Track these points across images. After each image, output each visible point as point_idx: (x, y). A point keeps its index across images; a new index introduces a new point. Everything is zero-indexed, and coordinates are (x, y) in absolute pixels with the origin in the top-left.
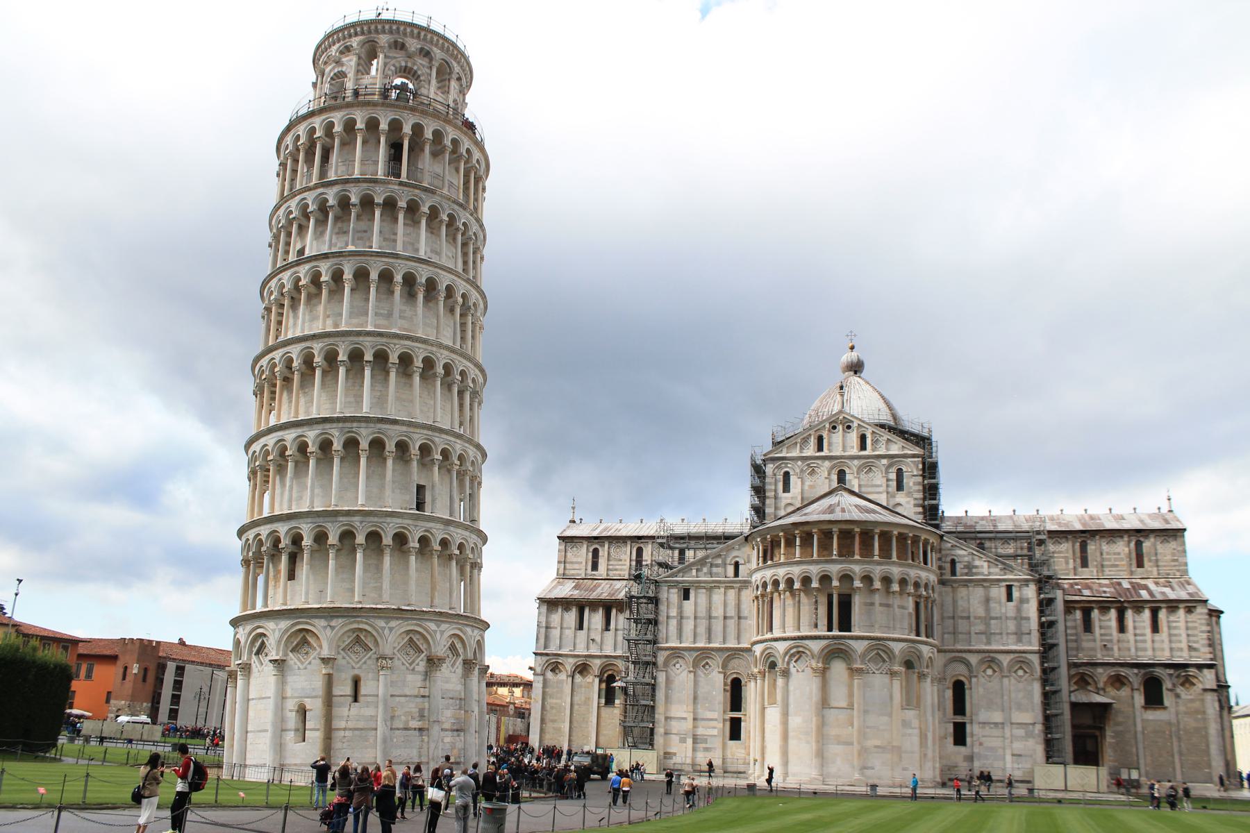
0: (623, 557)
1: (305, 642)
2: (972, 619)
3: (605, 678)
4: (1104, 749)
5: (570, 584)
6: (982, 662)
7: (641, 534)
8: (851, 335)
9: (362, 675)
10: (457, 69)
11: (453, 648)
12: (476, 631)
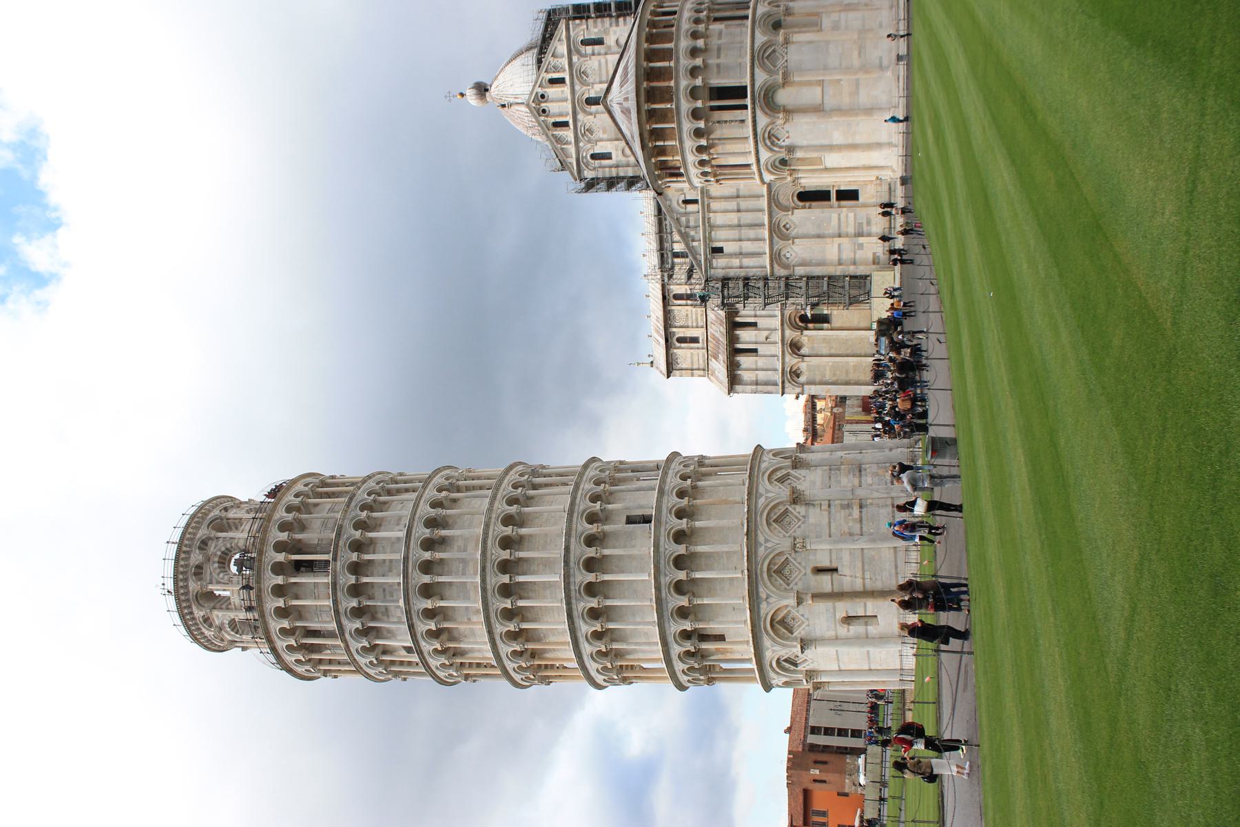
0: (684, 313)
1: (783, 622)
5: (713, 363)
7: (660, 296)
8: (449, 96)
10: (216, 512)
11: (781, 480)
12: (765, 458)
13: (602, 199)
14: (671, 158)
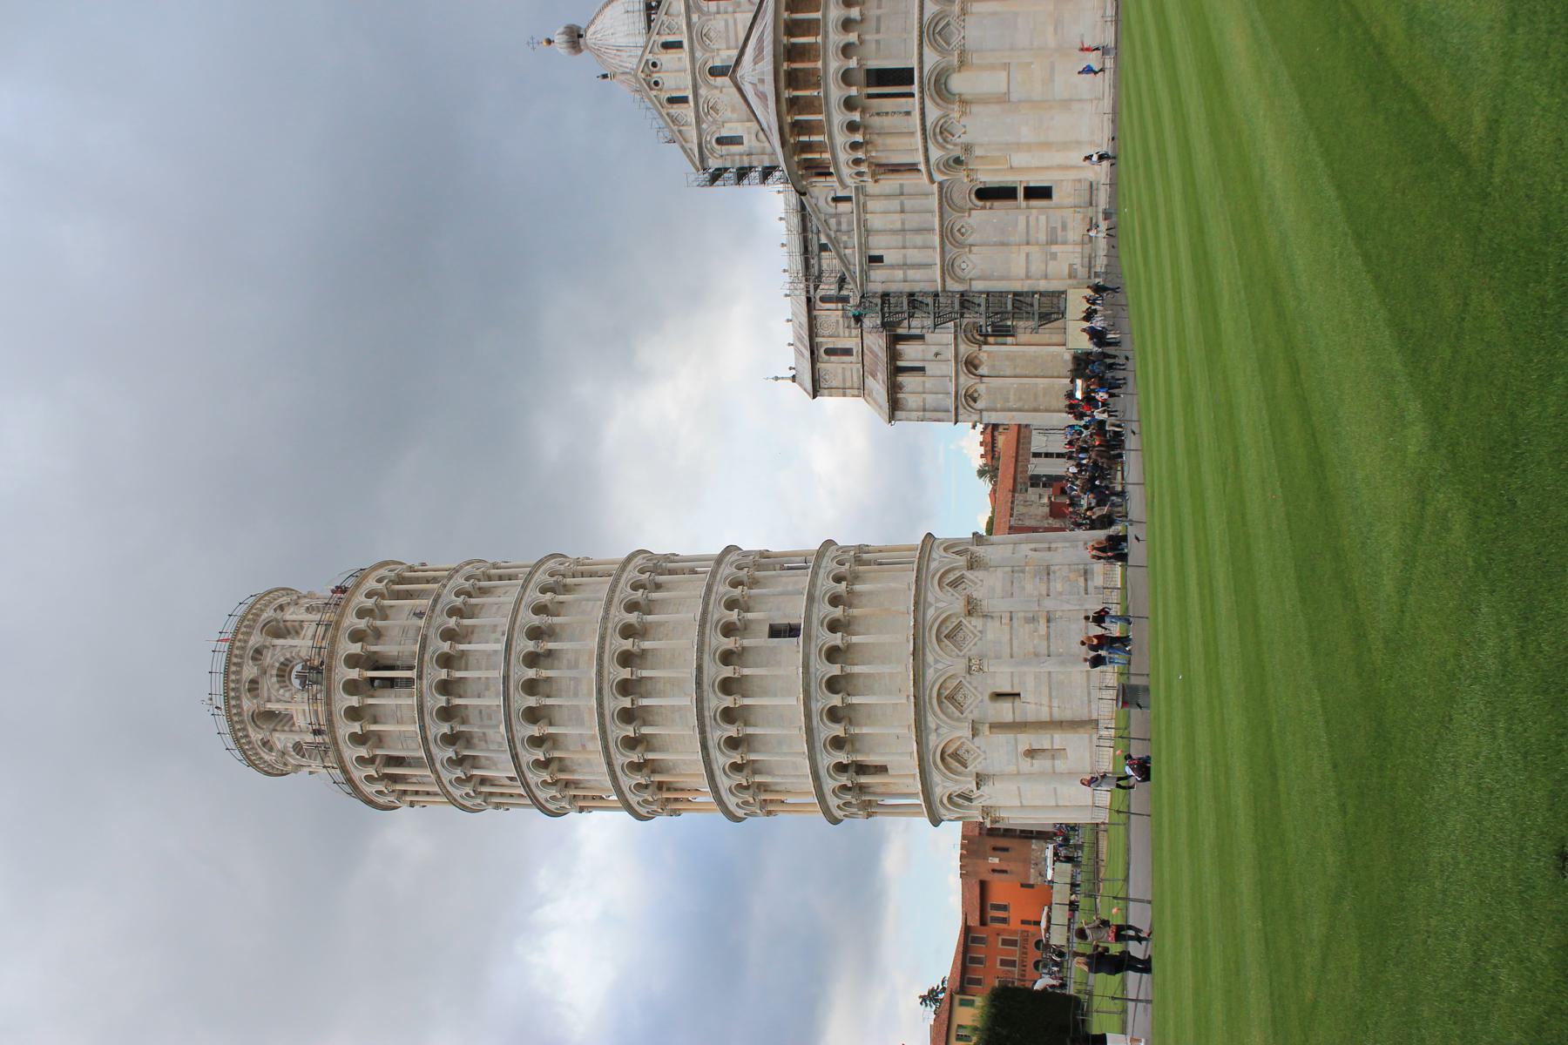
0: (833, 319)
3: (982, 338)
5: (870, 381)
9: (990, 691)
10: (269, 614)
11: (954, 584)
12: (934, 555)
13: (725, 191)
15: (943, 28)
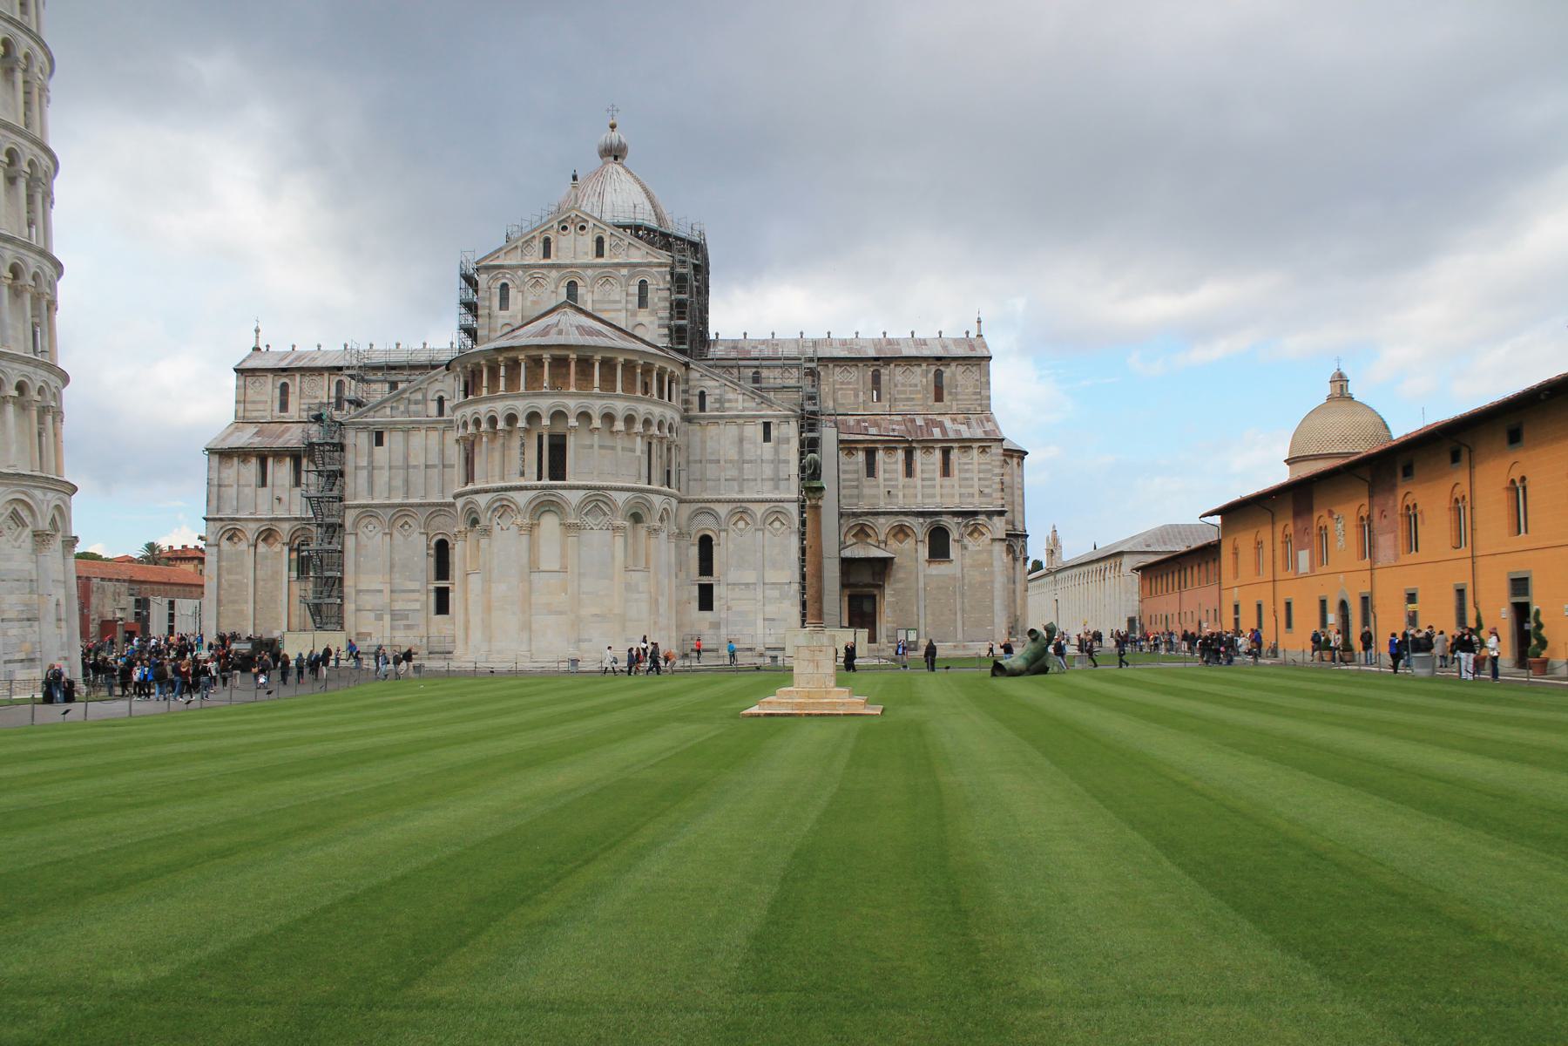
0: (319, 393)
2: (722, 462)
3: (295, 546)
4: (882, 611)
5: (252, 429)
6: (732, 513)
8: (613, 109)
11: (15, 516)
12: (50, 495)
13: (454, 290)
14: (485, 383)
15: (601, 509)
